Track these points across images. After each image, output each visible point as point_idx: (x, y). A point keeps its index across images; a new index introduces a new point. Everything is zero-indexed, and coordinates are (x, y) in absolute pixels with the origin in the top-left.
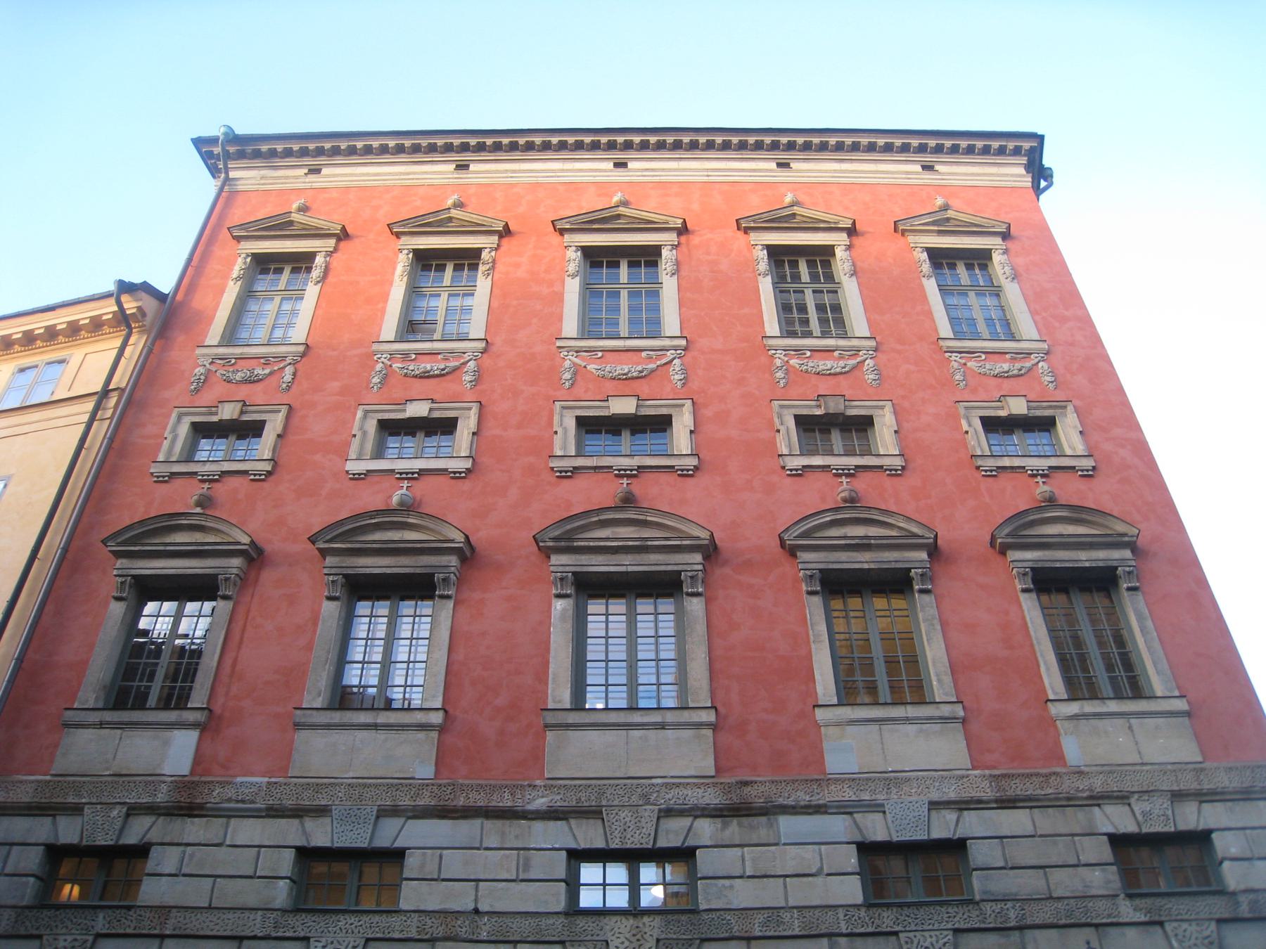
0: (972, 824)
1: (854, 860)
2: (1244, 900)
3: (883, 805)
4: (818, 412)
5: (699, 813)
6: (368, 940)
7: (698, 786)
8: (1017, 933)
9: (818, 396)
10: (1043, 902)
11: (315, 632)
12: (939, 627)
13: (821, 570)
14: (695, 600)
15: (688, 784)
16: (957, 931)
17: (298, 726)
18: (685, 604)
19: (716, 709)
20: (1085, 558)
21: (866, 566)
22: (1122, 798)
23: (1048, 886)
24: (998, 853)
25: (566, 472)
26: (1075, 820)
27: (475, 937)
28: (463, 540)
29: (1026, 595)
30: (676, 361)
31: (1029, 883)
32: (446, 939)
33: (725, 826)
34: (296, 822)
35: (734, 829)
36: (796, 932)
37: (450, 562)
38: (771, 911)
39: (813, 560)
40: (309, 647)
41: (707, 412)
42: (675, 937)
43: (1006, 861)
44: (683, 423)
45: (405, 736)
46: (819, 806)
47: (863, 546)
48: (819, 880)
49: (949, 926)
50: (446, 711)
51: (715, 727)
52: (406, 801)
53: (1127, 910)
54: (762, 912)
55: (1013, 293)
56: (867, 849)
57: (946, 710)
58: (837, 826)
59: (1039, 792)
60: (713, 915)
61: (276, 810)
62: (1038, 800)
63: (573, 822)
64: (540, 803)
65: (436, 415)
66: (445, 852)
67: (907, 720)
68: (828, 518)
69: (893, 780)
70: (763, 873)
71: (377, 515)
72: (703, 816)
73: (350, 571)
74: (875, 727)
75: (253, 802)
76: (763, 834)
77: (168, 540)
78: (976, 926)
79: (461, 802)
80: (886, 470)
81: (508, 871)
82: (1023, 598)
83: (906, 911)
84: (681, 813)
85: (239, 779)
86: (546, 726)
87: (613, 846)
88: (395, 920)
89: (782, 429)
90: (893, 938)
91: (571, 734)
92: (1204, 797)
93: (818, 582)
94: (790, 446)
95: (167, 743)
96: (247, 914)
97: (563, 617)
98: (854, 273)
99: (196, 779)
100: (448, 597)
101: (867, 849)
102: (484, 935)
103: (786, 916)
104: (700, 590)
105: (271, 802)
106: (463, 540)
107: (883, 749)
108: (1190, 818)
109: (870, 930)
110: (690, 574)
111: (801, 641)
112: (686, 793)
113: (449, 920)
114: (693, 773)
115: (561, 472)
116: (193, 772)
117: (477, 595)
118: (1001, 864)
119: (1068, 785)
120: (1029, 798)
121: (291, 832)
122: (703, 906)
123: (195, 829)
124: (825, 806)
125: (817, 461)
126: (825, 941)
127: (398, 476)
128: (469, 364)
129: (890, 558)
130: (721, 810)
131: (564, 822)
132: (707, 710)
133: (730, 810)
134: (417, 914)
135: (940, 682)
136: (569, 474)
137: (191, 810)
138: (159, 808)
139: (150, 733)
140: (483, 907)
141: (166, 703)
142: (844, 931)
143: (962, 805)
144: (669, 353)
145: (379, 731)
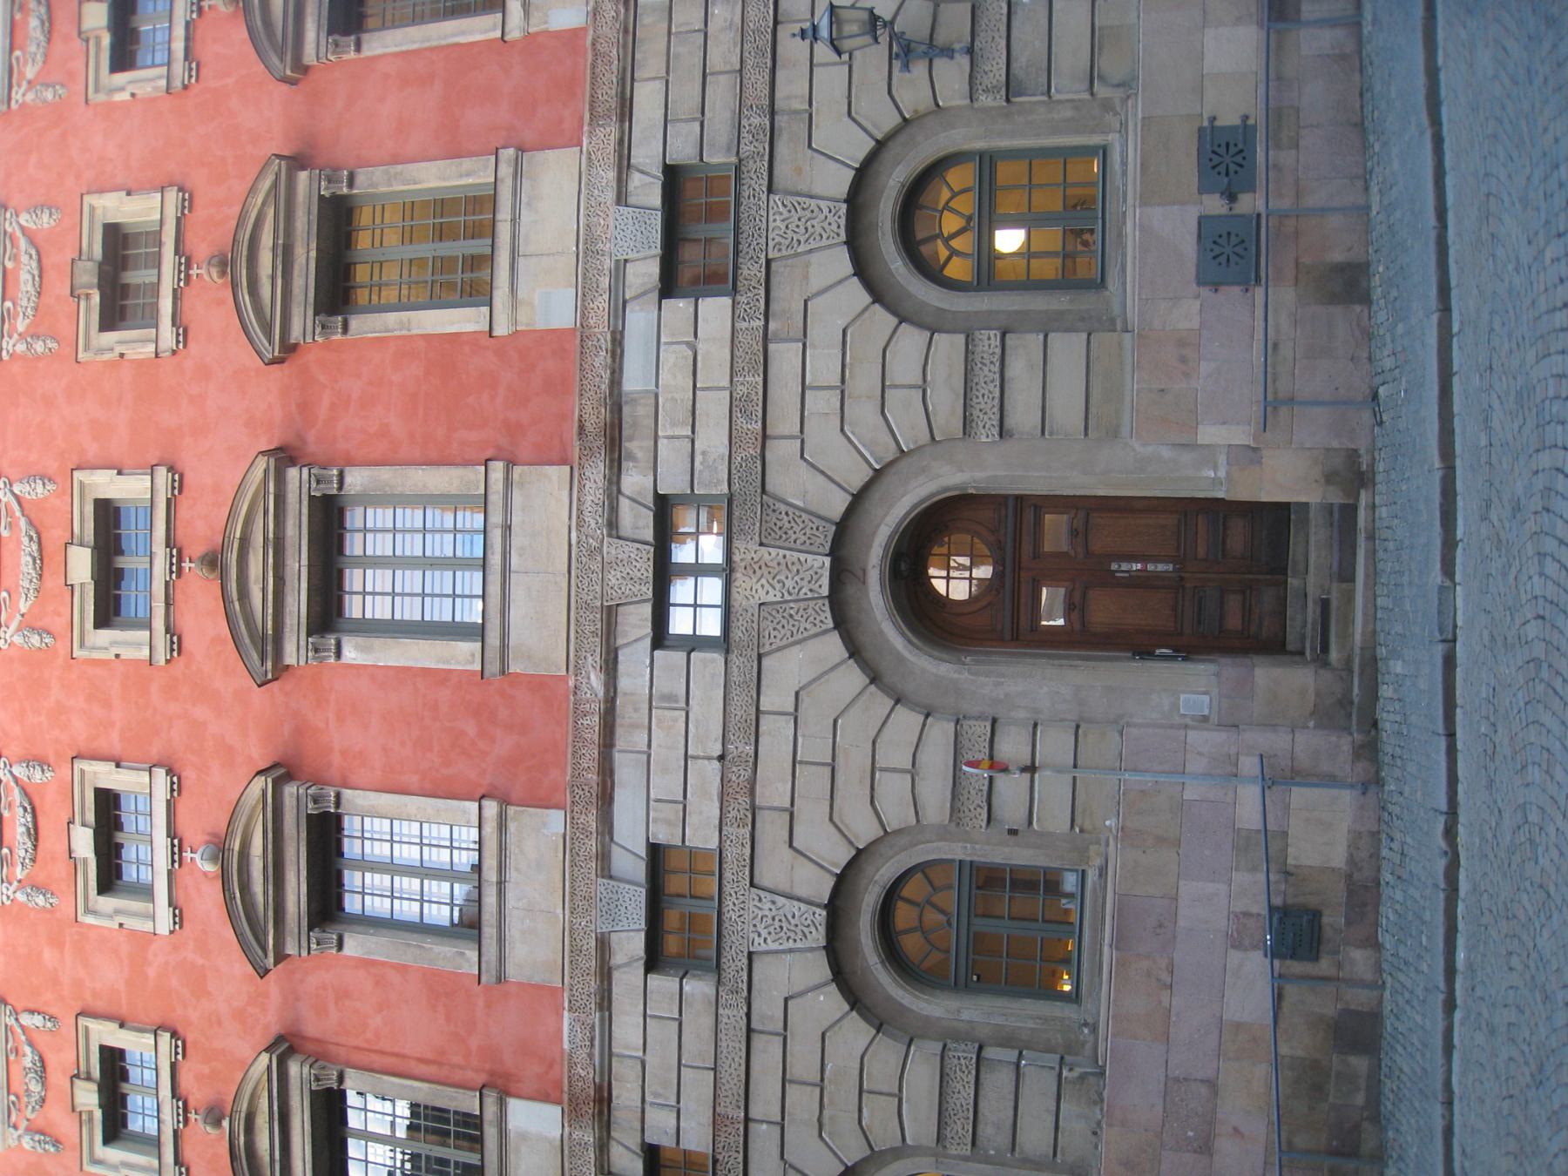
0: (647, 154)
3: (617, 261)
4: (96, 298)
5: (615, 488)
6: (752, 884)
8: (777, 118)
9: (72, 295)
10: (745, 81)
11: (383, 964)
12: (399, 167)
13: (316, 313)
14: (348, 480)
15: (579, 500)
16: (770, 190)
17: (501, 978)
18: (352, 493)
19: (487, 460)
21: (313, 254)
23: (726, 72)
24: (684, 128)
25: (172, 643)
27: (752, 760)
28: (263, 778)
29: (365, 47)
31: (721, 94)
32: (752, 792)
33: (632, 457)
34: (616, 975)
35: (636, 446)
36: (760, 380)
37: (292, 794)
38: (734, 409)
39: (301, 322)
40: (402, 969)
41: (92, 450)
42: (758, 525)
43: (694, 120)
44: (106, 484)
45: (513, 847)
46: (614, 340)
47: (286, 255)
48: (701, 347)
49: (764, 197)
50: (483, 797)
51: (511, 463)
52: (592, 845)
54: (734, 418)
56: (669, 286)
57: (506, 171)
58: (639, 321)
59: (614, 67)
60: (735, 477)
61: (602, 999)
62: (624, 69)
63: (620, 642)
64: (596, 681)
65: (91, 817)
66: (652, 796)
67: (515, 221)
68: (246, 299)
69: (587, 247)
70: (690, 414)
71: (229, 890)
72: (618, 483)
73: (305, 923)
74: (522, 262)
75: (593, 1028)
76: (643, 411)
77: (267, 1159)
78: (766, 166)
79: (593, 777)
80: (183, 213)
81: (675, 720)
82: (367, 52)
83: (743, 247)
84: (614, 510)
85: (566, 1046)
86: (503, 672)
87: (650, 594)
88: (731, 853)
89: (119, 349)
90: (774, 265)
93: (332, 319)
94: (145, 341)
95: (524, 1136)
96: (721, 1026)
97: (366, 650)
99: (566, 1097)
100: (338, 796)
101: (669, 286)
102: (750, 749)
103: (741, 390)
104: (335, 472)
105: (593, 1006)
106: (263, 778)
107: (548, 255)
109: (762, 292)
110: (314, 485)
111: (407, 347)
112: (590, 503)
113: (730, 790)
114: (566, 493)
115: (172, 650)
116: (558, 1102)
117: (336, 759)
118: (697, 126)
119: (609, 31)
121: (628, 979)
122: (724, 489)
123: (625, 1095)
124: (613, 333)
126: (772, 347)
127: (176, 865)
128: (17, 775)
130: (612, 461)
131: (620, 653)
132: (490, 471)
133: (612, 451)
134: (724, 828)
135: (469, 174)
136: (175, 639)
137: (603, 1100)
138: (600, 1138)
139: (512, 1157)
140: (717, 750)
141: (477, 1142)
142: (762, 323)
143: (624, 164)
145: (507, 879)
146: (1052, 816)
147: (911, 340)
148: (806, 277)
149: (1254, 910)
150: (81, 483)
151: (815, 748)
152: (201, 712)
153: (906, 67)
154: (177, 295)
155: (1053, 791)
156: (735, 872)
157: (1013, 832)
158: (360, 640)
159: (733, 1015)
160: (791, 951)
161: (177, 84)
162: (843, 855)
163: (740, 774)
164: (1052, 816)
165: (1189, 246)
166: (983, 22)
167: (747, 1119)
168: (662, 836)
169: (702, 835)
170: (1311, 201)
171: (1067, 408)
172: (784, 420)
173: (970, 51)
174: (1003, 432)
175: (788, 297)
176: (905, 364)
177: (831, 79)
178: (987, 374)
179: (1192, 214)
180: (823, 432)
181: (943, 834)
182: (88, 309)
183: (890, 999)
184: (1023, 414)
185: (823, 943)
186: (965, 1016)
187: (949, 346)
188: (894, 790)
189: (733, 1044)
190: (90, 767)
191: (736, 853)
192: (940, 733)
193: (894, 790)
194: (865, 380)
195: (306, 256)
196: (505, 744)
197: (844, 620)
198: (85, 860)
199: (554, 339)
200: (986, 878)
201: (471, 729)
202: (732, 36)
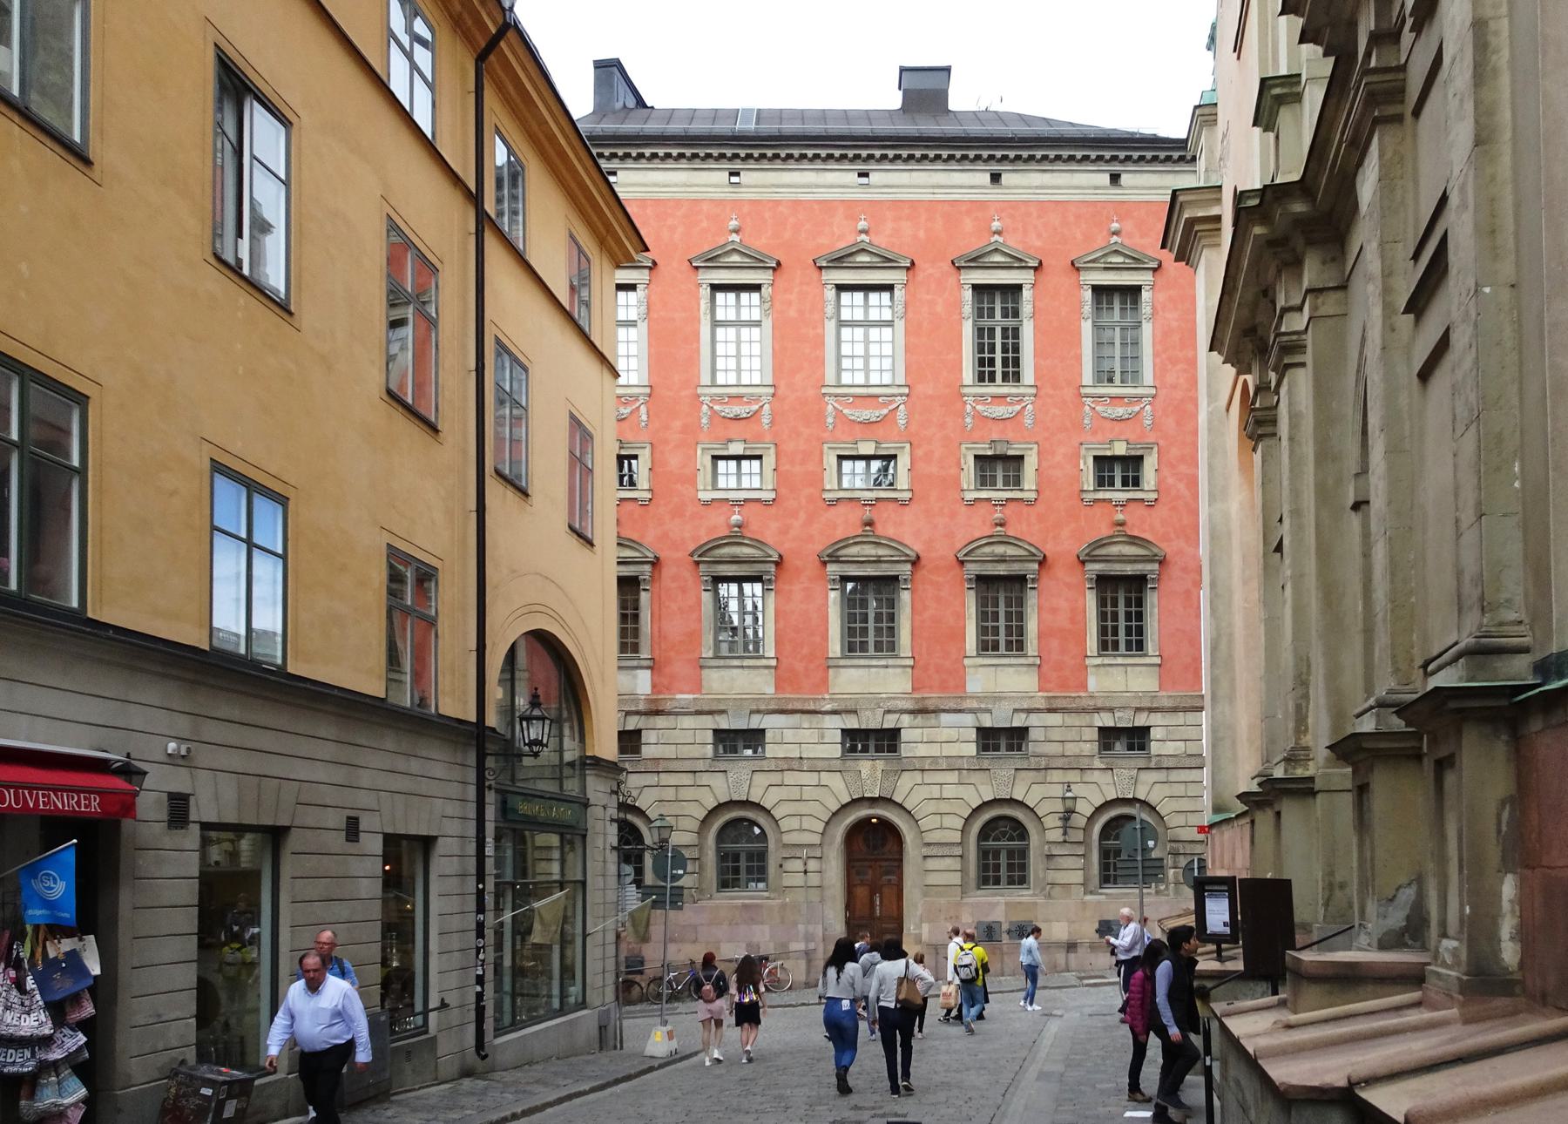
0: (1034, 720)
1: (974, 736)
2: (1154, 760)
7: (903, 699)
14: (906, 592)
16: (1016, 769)
17: (701, 667)
20: (1129, 569)
21: (1002, 573)
22: (1111, 710)
26: (1084, 719)
30: (902, 407)
31: (1054, 749)
33: (915, 718)
34: (710, 717)
35: (919, 720)
39: (973, 569)
40: (700, 620)
47: (1002, 560)
48: (958, 744)
51: (913, 667)
52: (763, 707)
53: (1097, 763)
55: (1147, 330)
56: (980, 730)
57: (1030, 661)
58: (969, 719)
64: (828, 707)
67: (1010, 665)
69: (997, 698)
74: (993, 669)
76: (933, 722)
79: (790, 707)
82: (1087, 591)
84: (895, 712)
88: (764, 762)
91: (842, 670)
92: (1151, 710)
95: (635, 677)
98: (1034, 316)
101: (980, 730)
103: (940, 761)
108: (1141, 720)
111: (962, 617)
116: (653, 693)
117: (787, 587)
119: (1085, 703)
120: (1064, 709)
121: (709, 722)
122: (903, 756)
123: (660, 721)
125: (984, 495)
129: (1016, 569)
140: (804, 756)
143: (1029, 711)
144: (897, 399)
146: (788, 880)
147: (959, 823)
148: (982, 784)
149: (761, 950)
150: (903, 448)
151: (808, 793)
152: (802, 516)
153: (1060, 819)
154: (989, 500)
155: (798, 880)
156: (757, 765)
157: (781, 866)
158: (839, 599)
159: (700, 766)
160: (729, 787)
161: (1084, 496)
162: (768, 806)
163: (795, 765)
164: (788, 880)
165: (990, 919)
166: (1075, 846)
167: (658, 772)
168: (769, 736)
169: (771, 751)
170: (1006, 957)
171: (933, 879)
172: (929, 777)
173: (1065, 841)
174: (925, 857)
175: (976, 778)
176: (949, 821)
177: (1058, 791)
178: (946, 851)
179: (1001, 919)
180: (924, 792)
181: (779, 840)
182: (983, 448)
183: (712, 824)
184: (932, 864)
185: (734, 799)
186: (710, 852)
187: (957, 837)
188: (793, 823)
189: (687, 766)
190: (772, 451)
191: (765, 765)
192: (816, 839)
193: (793, 823)
194: (944, 807)
195: (1001, 570)
196: (799, 666)
197: (855, 802)
198: (728, 449)
199: (962, 685)
200: (762, 856)
201: (805, 651)
202: (1077, 752)
